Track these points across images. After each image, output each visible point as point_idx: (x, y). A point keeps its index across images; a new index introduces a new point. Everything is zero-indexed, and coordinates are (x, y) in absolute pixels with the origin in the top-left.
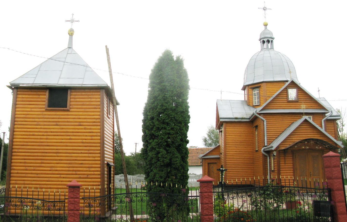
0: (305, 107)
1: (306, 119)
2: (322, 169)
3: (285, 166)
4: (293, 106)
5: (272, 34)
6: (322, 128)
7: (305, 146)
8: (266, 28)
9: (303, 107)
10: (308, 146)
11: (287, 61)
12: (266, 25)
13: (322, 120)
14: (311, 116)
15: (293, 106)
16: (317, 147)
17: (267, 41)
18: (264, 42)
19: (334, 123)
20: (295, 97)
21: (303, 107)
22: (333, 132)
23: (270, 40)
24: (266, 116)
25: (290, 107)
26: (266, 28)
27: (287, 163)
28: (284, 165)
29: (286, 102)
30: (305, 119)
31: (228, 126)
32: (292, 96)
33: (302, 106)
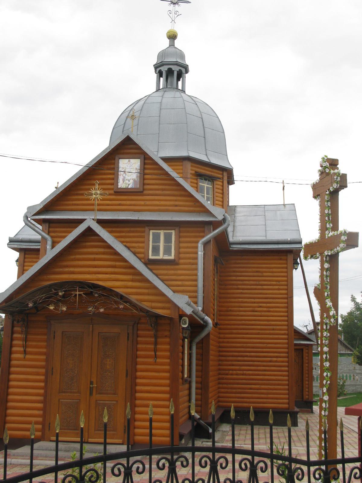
0: (92, 194)
1: (91, 226)
2: (127, 376)
3: (156, 363)
4: (128, 202)
5: (182, 56)
6: (53, 247)
7: (56, 305)
8: (172, 45)
9: (96, 194)
10: (64, 303)
11: (203, 114)
12: (172, 37)
13: (197, 242)
14: (173, 232)
15: (128, 202)
16: (90, 309)
17: (171, 71)
18: (160, 74)
19: (287, 260)
20: (134, 180)
21: (96, 194)
22: (283, 283)
23: (176, 69)
24: (57, 227)
25: (120, 205)
26: (172, 45)
27: (31, 353)
28: (21, 356)
29: (112, 192)
30: (87, 226)
31: (30, 260)
32: (127, 177)
33: (94, 192)
